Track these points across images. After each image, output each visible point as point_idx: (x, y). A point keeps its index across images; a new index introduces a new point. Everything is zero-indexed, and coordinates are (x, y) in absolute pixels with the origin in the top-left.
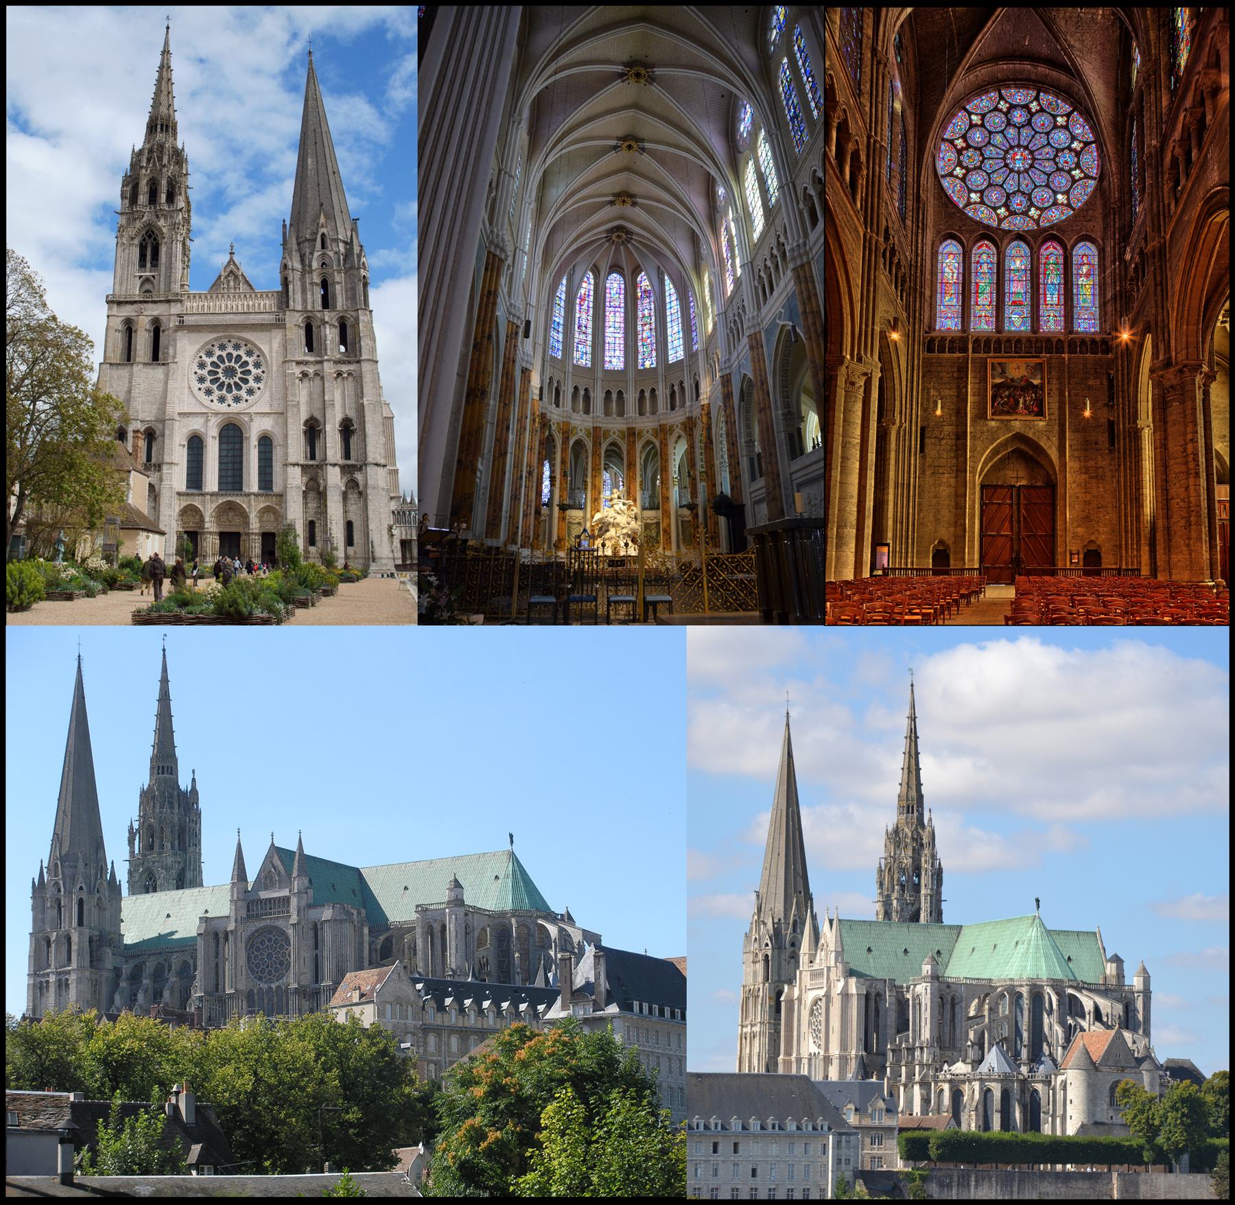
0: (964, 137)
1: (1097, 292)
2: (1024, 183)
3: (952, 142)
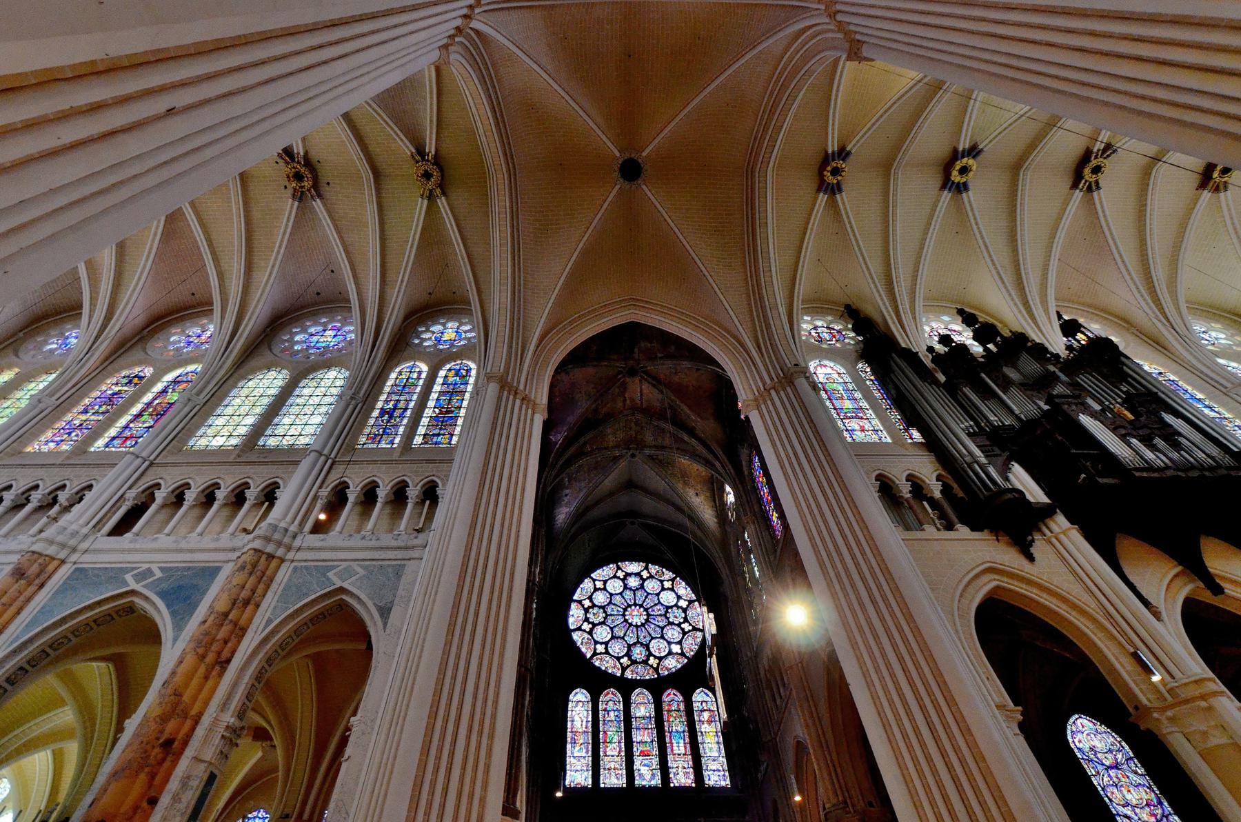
0: (590, 598)
1: (721, 740)
2: (642, 635)
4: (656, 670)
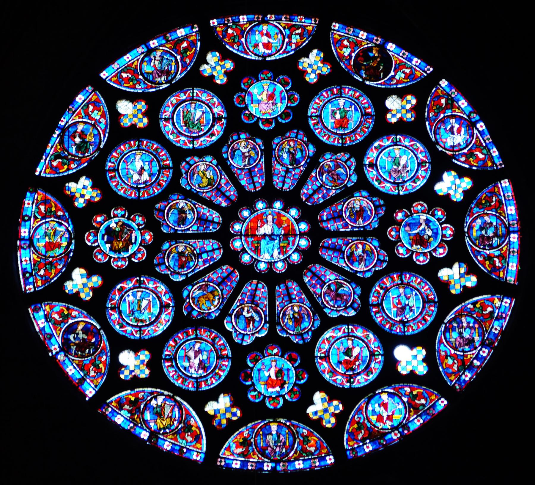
3: (56, 187)
4: (333, 437)
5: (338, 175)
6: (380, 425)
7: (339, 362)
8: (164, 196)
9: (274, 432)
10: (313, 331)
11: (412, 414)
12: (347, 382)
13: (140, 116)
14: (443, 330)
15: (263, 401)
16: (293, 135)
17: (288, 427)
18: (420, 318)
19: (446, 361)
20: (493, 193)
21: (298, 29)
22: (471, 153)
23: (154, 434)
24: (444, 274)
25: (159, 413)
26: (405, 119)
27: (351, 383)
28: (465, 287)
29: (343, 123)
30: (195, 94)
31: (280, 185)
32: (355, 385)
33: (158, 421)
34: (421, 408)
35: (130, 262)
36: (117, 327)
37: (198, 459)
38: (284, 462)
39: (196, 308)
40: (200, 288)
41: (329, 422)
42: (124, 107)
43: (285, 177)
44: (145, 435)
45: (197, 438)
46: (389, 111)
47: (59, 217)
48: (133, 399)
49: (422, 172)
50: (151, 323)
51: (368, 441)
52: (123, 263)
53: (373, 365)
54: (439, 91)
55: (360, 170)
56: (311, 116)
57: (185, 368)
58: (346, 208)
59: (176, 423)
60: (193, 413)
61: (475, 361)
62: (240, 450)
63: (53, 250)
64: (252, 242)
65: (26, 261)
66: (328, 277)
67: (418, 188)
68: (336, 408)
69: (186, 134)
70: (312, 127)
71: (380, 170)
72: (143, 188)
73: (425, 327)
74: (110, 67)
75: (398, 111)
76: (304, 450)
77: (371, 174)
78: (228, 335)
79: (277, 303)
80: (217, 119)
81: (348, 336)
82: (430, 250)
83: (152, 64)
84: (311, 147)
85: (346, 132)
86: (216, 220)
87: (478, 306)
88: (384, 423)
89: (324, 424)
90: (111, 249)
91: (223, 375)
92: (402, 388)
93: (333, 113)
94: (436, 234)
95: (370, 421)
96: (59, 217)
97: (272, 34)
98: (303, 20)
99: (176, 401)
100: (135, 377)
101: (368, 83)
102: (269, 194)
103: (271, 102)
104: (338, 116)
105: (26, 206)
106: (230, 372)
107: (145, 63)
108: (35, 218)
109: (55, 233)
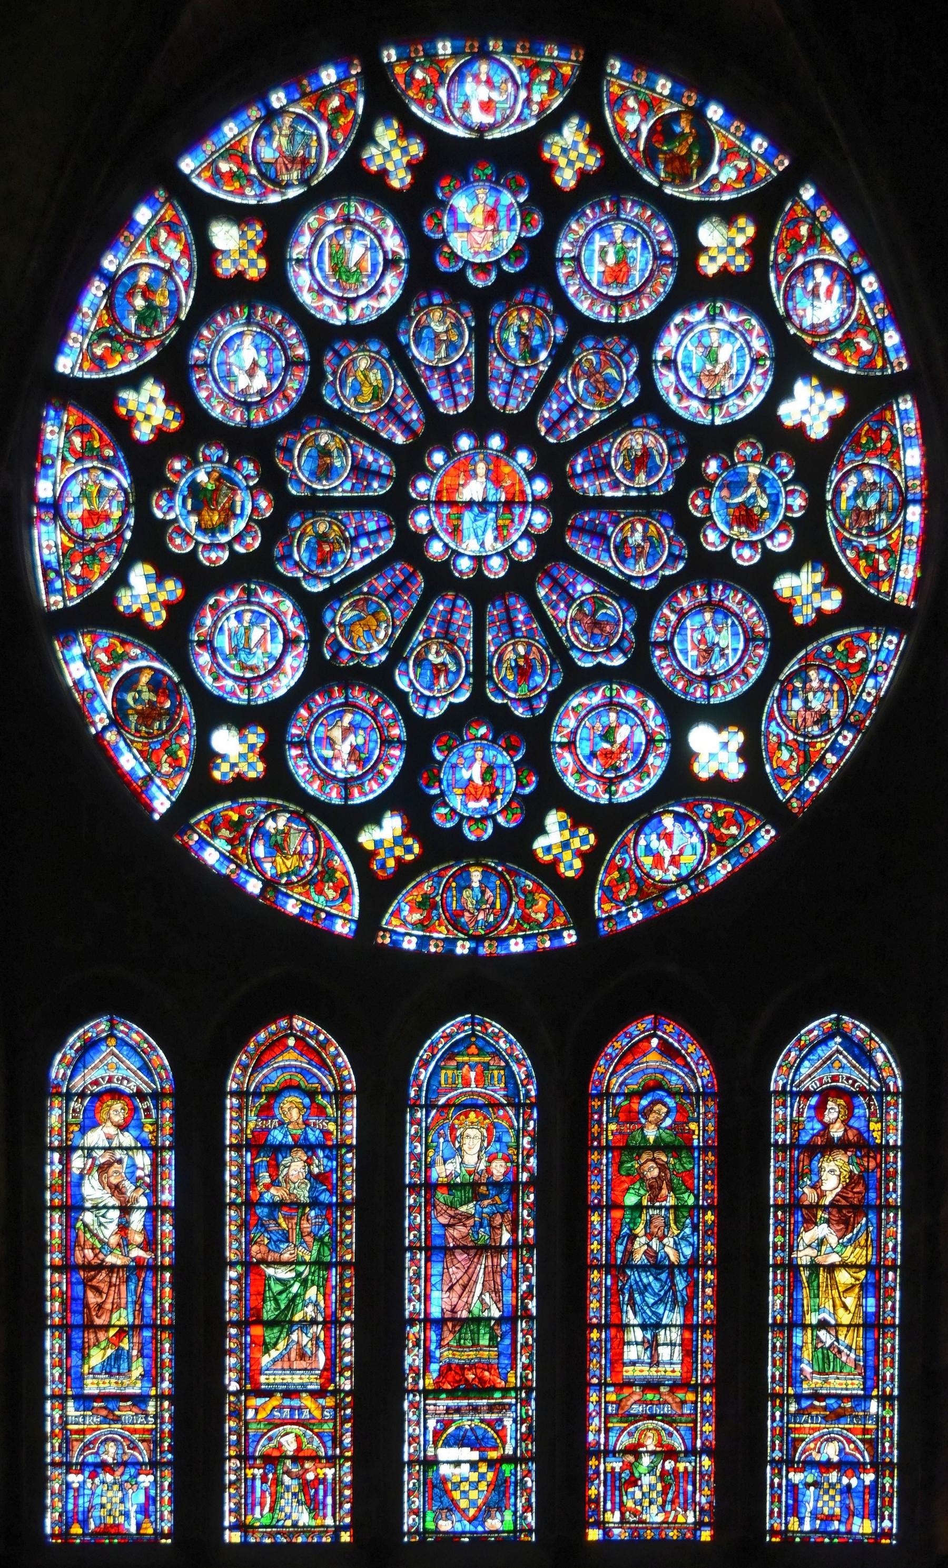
4: (575, 896)
5: (607, 381)
6: (658, 874)
7: (593, 755)
8: (294, 422)
9: (476, 884)
10: (550, 695)
11: (713, 853)
12: (605, 791)
13: (253, 254)
14: (776, 693)
15: (459, 826)
16: (528, 298)
17: (500, 875)
18: (738, 670)
19: (778, 754)
20: (882, 422)
21: (544, 71)
22: (847, 341)
23: (270, 884)
24: (784, 584)
25: (278, 847)
26: (733, 268)
27: (611, 794)
28: (819, 610)
29: (619, 273)
30: (353, 210)
31: (502, 400)
32: (620, 798)
33: (279, 859)
34: (729, 842)
35: (233, 553)
36: (208, 681)
37: (345, 931)
38: (491, 939)
39: (346, 646)
40: (354, 606)
41: (571, 867)
42: (224, 236)
43: (510, 384)
44: (254, 886)
45: (344, 893)
46: (705, 249)
47: (105, 460)
48: (235, 817)
49: (756, 379)
50: (269, 674)
51: (636, 904)
52: (220, 554)
53: (650, 760)
54: (798, 209)
55: (645, 375)
56: (562, 259)
57: (326, 761)
58: (618, 450)
59: (308, 863)
60: (339, 847)
61: (829, 756)
62: (417, 917)
63: (95, 525)
64: (448, 515)
65: (49, 547)
66: (579, 588)
67: (748, 411)
68: (584, 840)
69: (335, 292)
70: (563, 282)
71: (681, 373)
72: (257, 403)
73: (746, 688)
74: (199, 152)
75: (722, 250)
76: (526, 918)
77: (665, 380)
78: (400, 699)
79: (489, 637)
80: (391, 263)
81: (610, 704)
82: (763, 535)
83: (275, 144)
84: (559, 323)
85: (625, 293)
86: (385, 470)
87: (840, 648)
88: (666, 871)
89: (562, 870)
90: (199, 527)
91: (391, 775)
92: (699, 805)
93: (603, 251)
94: (774, 504)
95: (640, 867)
96: (105, 460)
97: (496, 79)
98: (555, 54)
99: (309, 823)
100: (240, 777)
101: (668, 190)
102: (481, 419)
103: (490, 227)
104: (611, 259)
105: (48, 436)
106: (403, 769)
107: (262, 143)
108: (64, 460)
109: (99, 492)
